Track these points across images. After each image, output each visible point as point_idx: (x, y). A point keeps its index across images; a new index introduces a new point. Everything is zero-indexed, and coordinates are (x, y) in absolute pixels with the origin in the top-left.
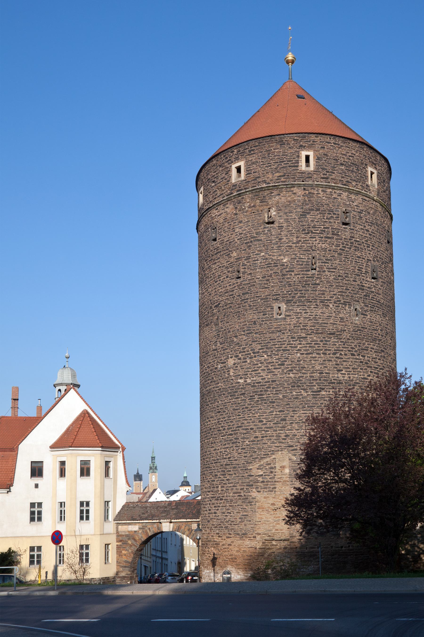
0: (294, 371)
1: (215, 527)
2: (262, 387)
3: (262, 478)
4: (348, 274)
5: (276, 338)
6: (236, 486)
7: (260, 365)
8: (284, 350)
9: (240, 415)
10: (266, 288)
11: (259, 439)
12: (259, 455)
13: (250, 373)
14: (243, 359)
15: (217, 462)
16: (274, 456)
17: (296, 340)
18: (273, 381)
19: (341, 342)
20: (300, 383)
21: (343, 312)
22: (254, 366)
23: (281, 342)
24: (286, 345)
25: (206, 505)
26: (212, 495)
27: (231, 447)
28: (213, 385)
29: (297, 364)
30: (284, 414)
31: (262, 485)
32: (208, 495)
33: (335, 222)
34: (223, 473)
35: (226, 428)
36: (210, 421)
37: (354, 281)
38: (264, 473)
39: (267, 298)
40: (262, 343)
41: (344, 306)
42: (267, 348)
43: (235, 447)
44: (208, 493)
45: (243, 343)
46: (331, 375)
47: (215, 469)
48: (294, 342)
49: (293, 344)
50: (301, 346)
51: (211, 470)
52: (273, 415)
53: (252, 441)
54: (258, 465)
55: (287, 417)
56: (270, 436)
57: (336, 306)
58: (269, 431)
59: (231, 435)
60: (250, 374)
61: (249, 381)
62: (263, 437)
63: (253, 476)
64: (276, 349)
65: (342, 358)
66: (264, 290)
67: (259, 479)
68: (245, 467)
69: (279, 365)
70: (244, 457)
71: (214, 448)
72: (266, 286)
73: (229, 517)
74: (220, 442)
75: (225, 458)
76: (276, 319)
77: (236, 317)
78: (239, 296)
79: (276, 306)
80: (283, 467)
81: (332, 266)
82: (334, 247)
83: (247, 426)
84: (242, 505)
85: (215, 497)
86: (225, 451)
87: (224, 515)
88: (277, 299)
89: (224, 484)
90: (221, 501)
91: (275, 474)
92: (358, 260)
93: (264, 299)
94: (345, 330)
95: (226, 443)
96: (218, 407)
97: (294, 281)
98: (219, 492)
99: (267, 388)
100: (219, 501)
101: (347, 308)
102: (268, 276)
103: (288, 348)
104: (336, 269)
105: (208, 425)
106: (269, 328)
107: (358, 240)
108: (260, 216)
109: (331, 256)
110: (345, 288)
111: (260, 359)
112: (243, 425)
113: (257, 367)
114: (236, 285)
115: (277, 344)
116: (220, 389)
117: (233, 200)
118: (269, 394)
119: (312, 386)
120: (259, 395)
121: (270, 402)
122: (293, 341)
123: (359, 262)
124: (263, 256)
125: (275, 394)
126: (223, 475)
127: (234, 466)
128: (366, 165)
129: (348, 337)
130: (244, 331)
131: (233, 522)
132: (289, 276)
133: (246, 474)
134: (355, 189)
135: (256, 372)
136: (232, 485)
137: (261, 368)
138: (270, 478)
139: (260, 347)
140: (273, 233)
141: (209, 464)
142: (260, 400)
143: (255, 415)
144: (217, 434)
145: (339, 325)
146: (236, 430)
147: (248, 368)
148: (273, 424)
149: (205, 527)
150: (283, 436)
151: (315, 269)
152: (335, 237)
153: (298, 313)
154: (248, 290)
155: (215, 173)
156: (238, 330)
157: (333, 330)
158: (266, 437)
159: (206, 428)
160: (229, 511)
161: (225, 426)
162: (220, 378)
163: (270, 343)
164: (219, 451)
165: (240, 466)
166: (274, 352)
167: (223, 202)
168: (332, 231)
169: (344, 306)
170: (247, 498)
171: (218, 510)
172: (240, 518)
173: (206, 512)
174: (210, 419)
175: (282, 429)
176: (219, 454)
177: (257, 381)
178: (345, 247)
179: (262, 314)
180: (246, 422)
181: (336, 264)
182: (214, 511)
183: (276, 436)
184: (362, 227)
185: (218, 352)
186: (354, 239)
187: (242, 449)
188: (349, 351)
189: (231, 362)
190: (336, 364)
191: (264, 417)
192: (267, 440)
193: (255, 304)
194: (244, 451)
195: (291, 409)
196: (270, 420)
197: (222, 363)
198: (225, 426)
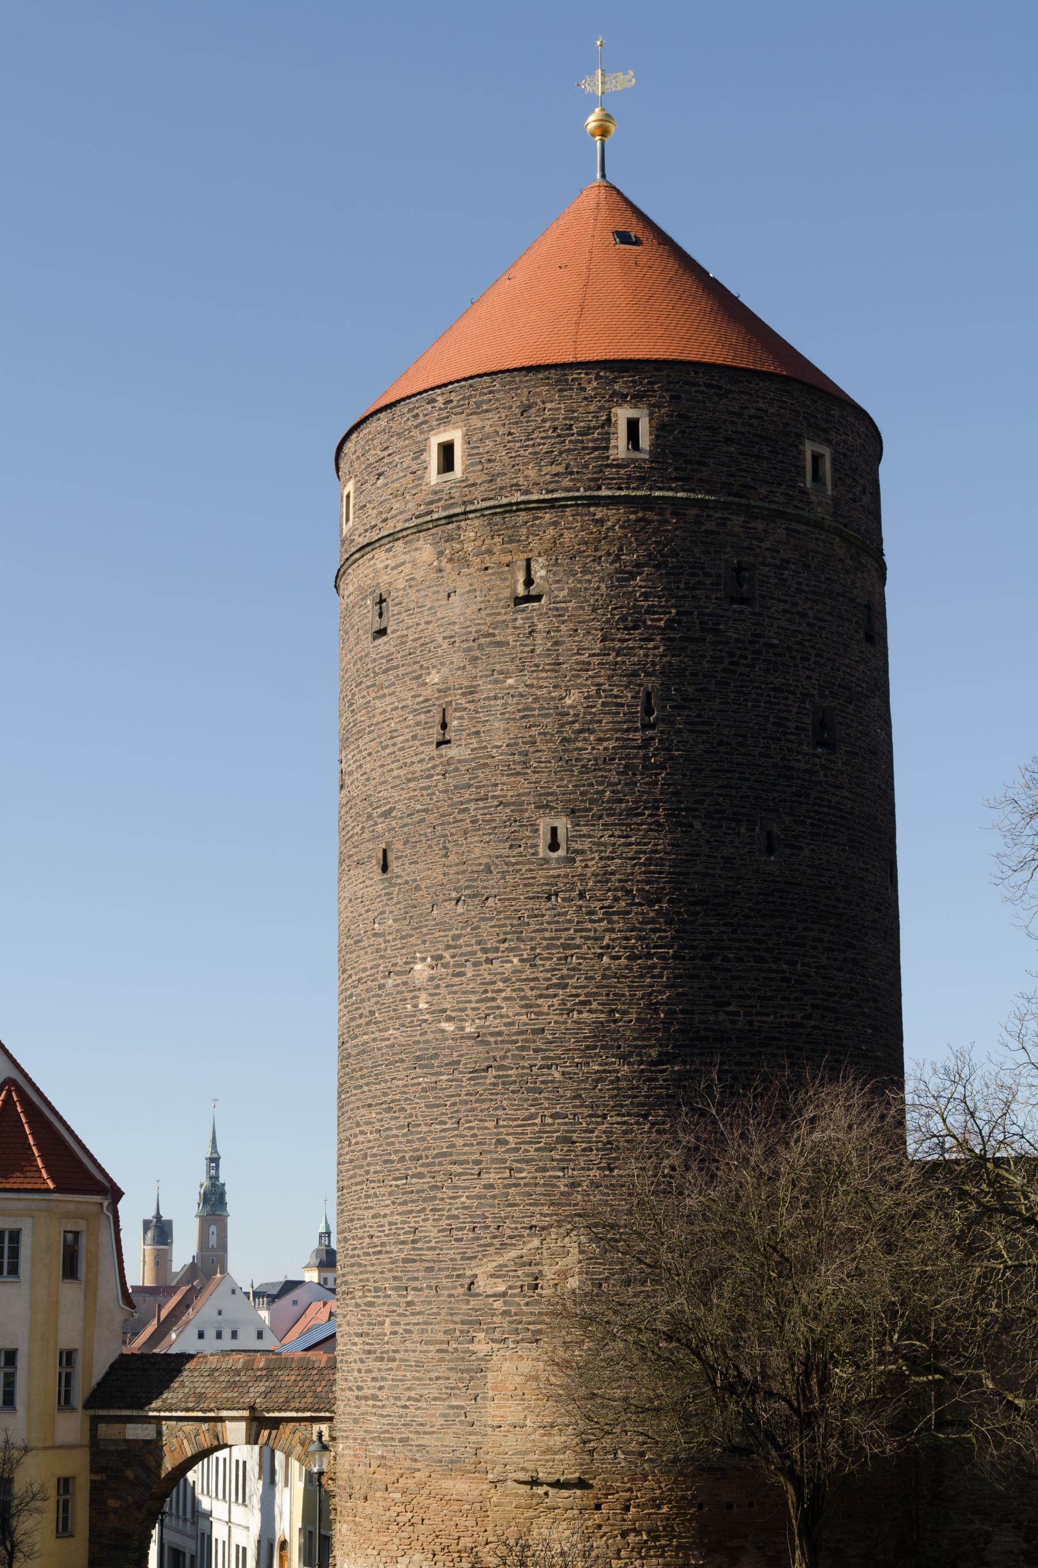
0: (594, 1005)
1: (373, 1439)
2: (506, 1046)
3: (505, 1303)
4: (745, 736)
5: (544, 912)
6: (431, 1324)
8: (565, 947)
9: (445, 1123)
10: (518, 774)
11: (496, 1192)
12: (494, 1237)
13: (473, 1005)
15: (380, 1252)
16: (536, 1242)
17: (600, 920)
18: (535, 1032)
19: (724, 925)
20: (612, 1040)
21: (732, 842)
22: (484, 987)
23: (558, 922)
24: (572, 932)
25: (348, 1371)
26: (368, 1344)
27: (419, 1212)
28: (373, 1033)
29: (603, 987)
30: (566, 1124)
32: (355, 1344)
33: (708, 597)
34: (396, 1284)
35: (407, 1156)
36: (362, 1132)
37: (761, 755)
38: (510, 1287)
39: (522, 803)
40: (505, 925)
41: (733, 825)
42: (519, 939)
43: (431, 1210)
44: (356, 1339)
46: (697, 1016)
47: (374, 1272)
48: (596, 925)
49: (590, 930)
50: (614, 936)
51: (366, 1272)
52: (535, 1124)
54: (495, 1264)
55: (574, 1132)
56: (526, 1185)
57: (713, 827)
58: (521, 1171)
59: (420, 1175)
60: (473, 1009)
62: (506, 1186)
64: (545, 943)
65: (729, 970)
66: (512, 779)
67: (496, 1305)
71: (372, 1212)
72: (519, 768)
73: (412, 1410)
74: (391, 1194)
75: (403, 1243)
76: (546, 861)
78: (446, 791)
80: (564, 1275)
81: (699, 716)
82: (706, 665)
83: (465, 1154)
84: (448, 1378)
85: (375, 1352)
86: (403, 1222)
87: (399, 1403)
88: (547, 806)
89: (400, 1315)
90: (391, 1365)
92: (775, 697)
93: (513, 804)
94: (739, 892)
95: (405, 1197)
96: (385, 1094)
97: (596, 759)
98: (386, 1338)
99: (522, 1048)
100: (384, 1365)
101: (743, 830)
102: (523, 743)
103: (578, 941)
104: (710, 724)
105: (357, 1143)
106: (525, 885)
107: (775, 641)
109: (697, 690)
110: (737, 775)
111: (500, 970)
112: (454, 1150)
113: (493, 991)
114: (438, 761)
115: (546, 930)
117: (434, 531)
119: (645, 1047)
120: (500, 1068)
121: (529, 1090)
122: (592, 921)
123: (778, 704)
124: (511, 687)
125: (541, 1067)
126: (397, 1289)
128: (799, 436)
129: (746, 910)
131: (422, 1425)
132: (579, 744)
134: (767, 505)
135: (489, 1004)
136: (421, 1319)
137: (503, 995)
138: (527, 1304)
140: (540, 626)
141: (359, 1256)
142: (500, 1081)
143: (487, 1124)
144: (381, 1172)
145: (720, 877)
146: (433, 1164)
148: (536, 1150)
149: (347, 1437)
151: (652, 726)
152: (710, 637)
153: (604, 844)
154: (470, 779)
155: (386, 453)
157: (704, 890)
159: (353, 1151)
160: (413, 1394)
161: (406, 1152)
162: (392, 1014)
163: (528, 924)
164: (386, 1220)
165: (443, 1265)
166: (538, 951)
167: (405, 533)
168: (700, 623)
169: (733, 825)
170: (463, 1359)
171: (381, 1388)
172: (445, 1415)
173: (348, 1393)
174: (364, 1128)
176: (386, 1228)
177: (492, 1029)
178: (737, 664)
180: (460, 1142)
181: (711, 710)
182: (372, 1391)
183: (544, 1185)
184: (787, 607)
185: (389, 941)
186: (762, 641)
187: (449, 1217)
188: (749, 949)
190: (712, 987)
191: (511, 1130)
192: (518, 1194)
193: (488, 817)
195: (586, 1112)
197: (397, 974)
198: (406, 1152)
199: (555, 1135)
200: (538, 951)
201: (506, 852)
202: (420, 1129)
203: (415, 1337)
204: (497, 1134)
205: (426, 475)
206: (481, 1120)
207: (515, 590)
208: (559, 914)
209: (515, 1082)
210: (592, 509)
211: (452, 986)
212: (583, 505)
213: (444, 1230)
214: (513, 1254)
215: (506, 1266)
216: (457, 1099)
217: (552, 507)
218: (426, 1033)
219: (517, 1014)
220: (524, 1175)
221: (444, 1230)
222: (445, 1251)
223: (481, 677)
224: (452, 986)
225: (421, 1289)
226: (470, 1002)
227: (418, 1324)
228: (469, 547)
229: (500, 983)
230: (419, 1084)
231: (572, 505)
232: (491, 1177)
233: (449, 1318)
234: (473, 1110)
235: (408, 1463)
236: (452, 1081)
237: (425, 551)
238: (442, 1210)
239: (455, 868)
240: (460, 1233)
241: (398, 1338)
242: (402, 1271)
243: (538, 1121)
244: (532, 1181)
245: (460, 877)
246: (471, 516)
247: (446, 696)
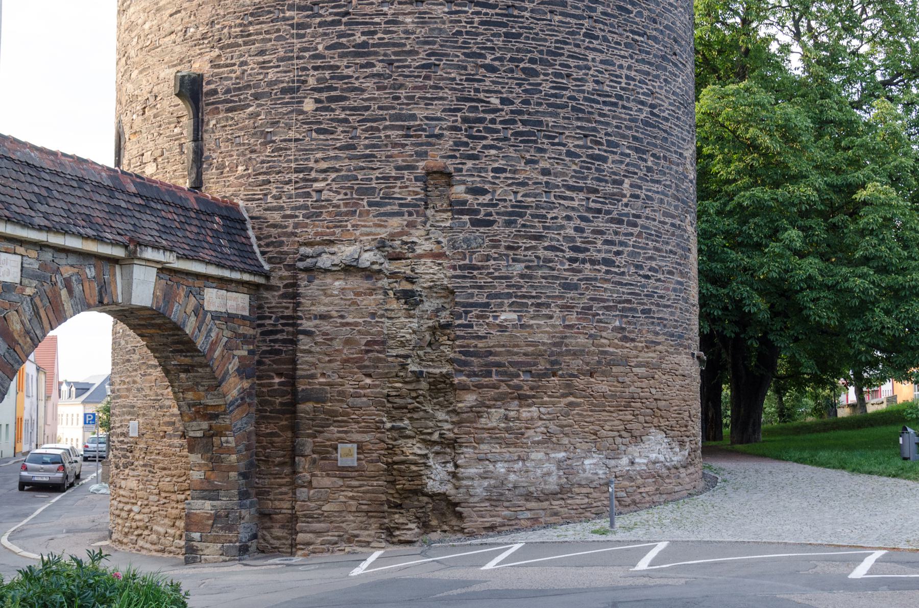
1: (607, 308)
90: (630, 229)
98: (625, 200)
100: (624, 229)
126: (637, 150)
160: (654, 264)
164: (625, 72)
171: (618, 253)
203: (656, 205)
235: (651, 337)
241: (640, 203)
242: (642, 133)
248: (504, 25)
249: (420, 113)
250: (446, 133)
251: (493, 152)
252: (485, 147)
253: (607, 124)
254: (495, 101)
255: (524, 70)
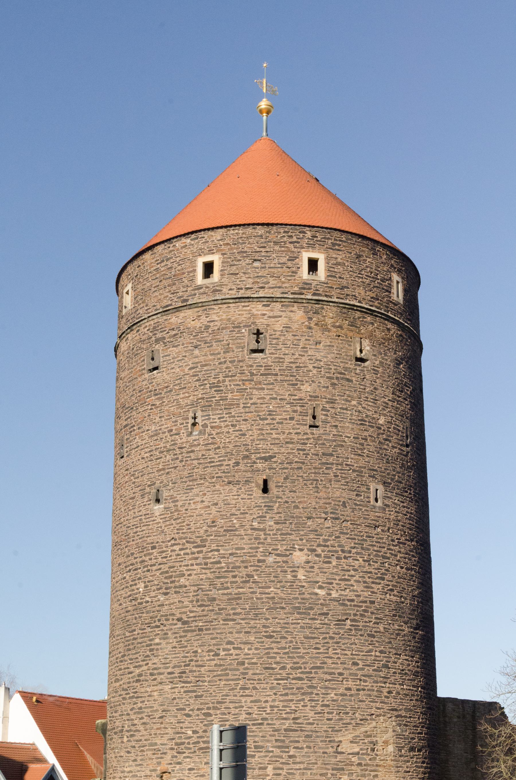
0: (395, 592)
2: (356, 608)
3: (359, 758)
6: (310, 769)
7: (352, 573)
9: (319, 649)
10: (359, 455)
11: (353, 692)
12: (352, 719)
13: (337, 582)
14: (325, 557)
16: (374, 724)
17: (396, 546)
22: (343, 573)
27: (299, 701)
31: (359, 771)
35: (288, 666)
40: (354, 539)
43: (309, 701)
45: (324, 531)
52: (371, 655)
53: (342, 695)
54: (353, 735)
56: (368, 690)
60: (337, 584)
61: (334, 594)
62: (358, 690)
63: (343, 753)
64: (375, 553)
66: (356, 457)
67: (353, 759)
68: (330, 737)
69: (378, 578)
70: (328, 719)
72: (360, 452)
75: (285, 719)
77: (310, 486)
79: (372, 486)
80: (386, 743)
83: (333, 668)
89: (283, 763)
91: (378, 753)
99: (365, 611)
102: (362, 439)
103: (388, 555)
106: (364, 518)
108: (350, 345)
111: (353, 564)
112: (325, 666)
113: (349, 576)
115: (375, 546)
116: (273, 598)
117: (305, 305)
118: (366, 622)
124: (355, 406)
127: (307, 733)
130: (326, 513)
133: (331, 750)
135: (346, 583)
136: (302, 766)
137: (355, 578)
138: (370, 760)
139: (353, 545)
140: (367, 377)
142: (353, 628)
143: (346, 652)
146: (311, 673)
147: (332, 573)
148: (374, 670)
150: (385, 690)
156: (315, 508)
158: (364, 690)
163: (366, 541)
164: (268, 705)
165: (319, 734)
166: (372, 557)
167: (283, 300)
175: (385, 680)
177: (348, 598)
179: (355, 493)
180: (330, 661)
183: (377, 691)
187: (323, 706)
189: (299, 557)
191: (360, 657)
193: (344, 475)
194: (326, 710)
196: (368, 663)
198: (286, 663)
199: (381, 663)
200: (372, 557)
201: (354, 497)
202: (299, 651)
204: (352, 659)
205: (299, 272)
206: (343, 650)
207: (355, 353)
208: (380, 538)
209: (361, 630)
210: (386, 322)
211: (323, 568)
212: (383, 318)
213: (320, 713)
214: (363, 729)
215: (359, 737)
216: (328, 636)
217: (372, 314)
218: (304, 594)
219: (362, 591)
220: (367, 684)
221: (320, 713)
222: (320, 726)
223: (338, 395)
224: (323, 568)
225: (302, 748)
226: (335, 579)
227: (300, 769)
228: (329, 321)
229: (352, 572)
230: (299, 624)
231: (379, 317)
232: (350, 684)
233: (323, 766)
234: (338, 643)
236: (324, 624)
237: (298, 315)
238: (318, 701)
239: (324, 501)
240: (331, 715)
242: (284, 737)
243: (373, 653)
244: (371, 688)
245: (327, 506)
246: (331, 304)
247: (316, 401)
248: (194, 691)
249: (159, 742)
250: (169, 751)
251: (188, 760)
252: (185, 757)
253: (255, 736)
254: (190, 733)
255: (204, 714)
